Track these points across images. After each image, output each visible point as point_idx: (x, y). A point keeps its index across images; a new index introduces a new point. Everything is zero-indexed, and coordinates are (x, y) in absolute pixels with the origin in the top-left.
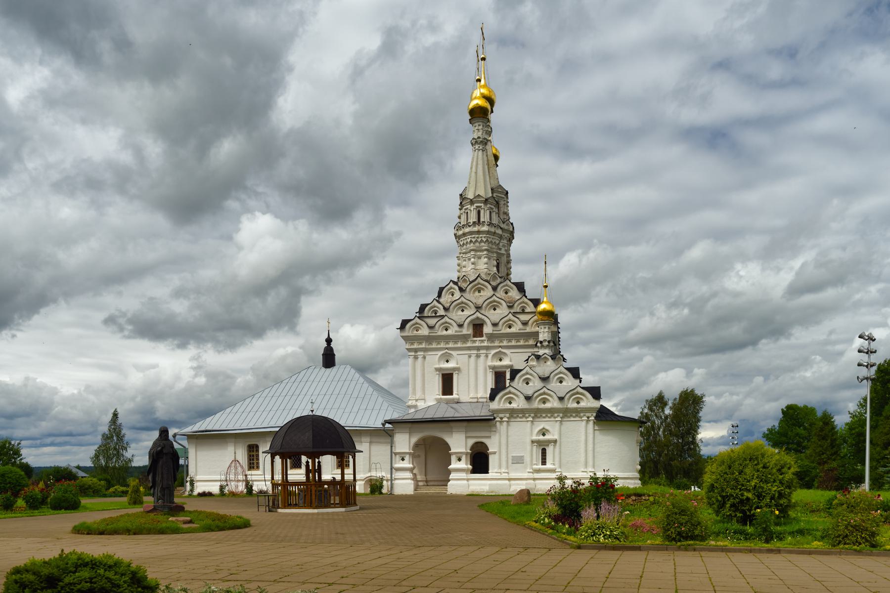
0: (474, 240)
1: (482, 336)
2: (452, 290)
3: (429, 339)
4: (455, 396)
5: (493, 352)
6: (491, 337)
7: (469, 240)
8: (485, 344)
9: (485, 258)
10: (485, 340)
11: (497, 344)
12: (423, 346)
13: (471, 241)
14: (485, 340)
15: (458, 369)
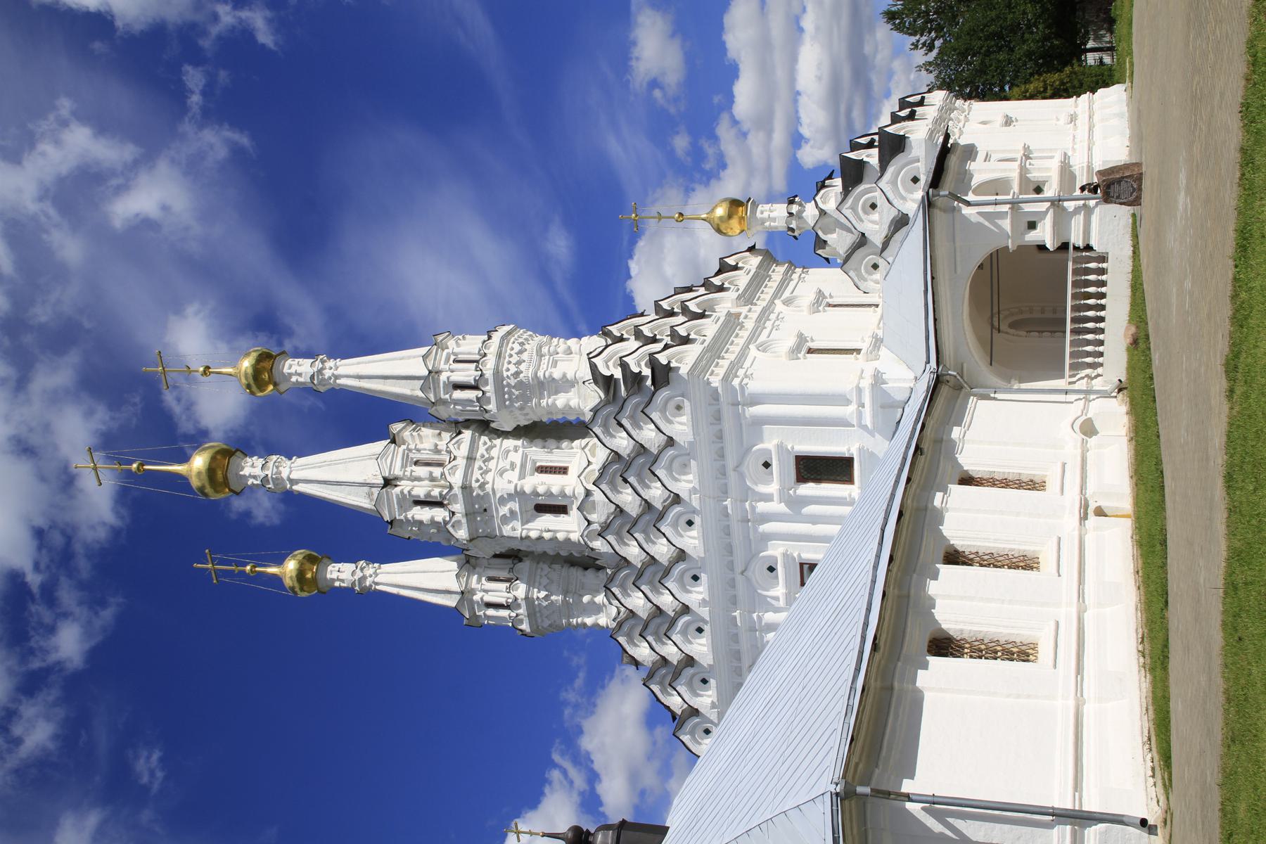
0: (520, 340)
1: (740, 314)
2: (611, 364)
3: (715, 350)
4: (864, 346)
5: (779, 305)
6: (748, 297)
7: (517, 347)
8: (757, 309)
9: (566, 344)
10: (750, 309)
11: (761, 304)
12: (725, 364)
13: (522, 344)
14: (750, 309)
15: (802, 338)
